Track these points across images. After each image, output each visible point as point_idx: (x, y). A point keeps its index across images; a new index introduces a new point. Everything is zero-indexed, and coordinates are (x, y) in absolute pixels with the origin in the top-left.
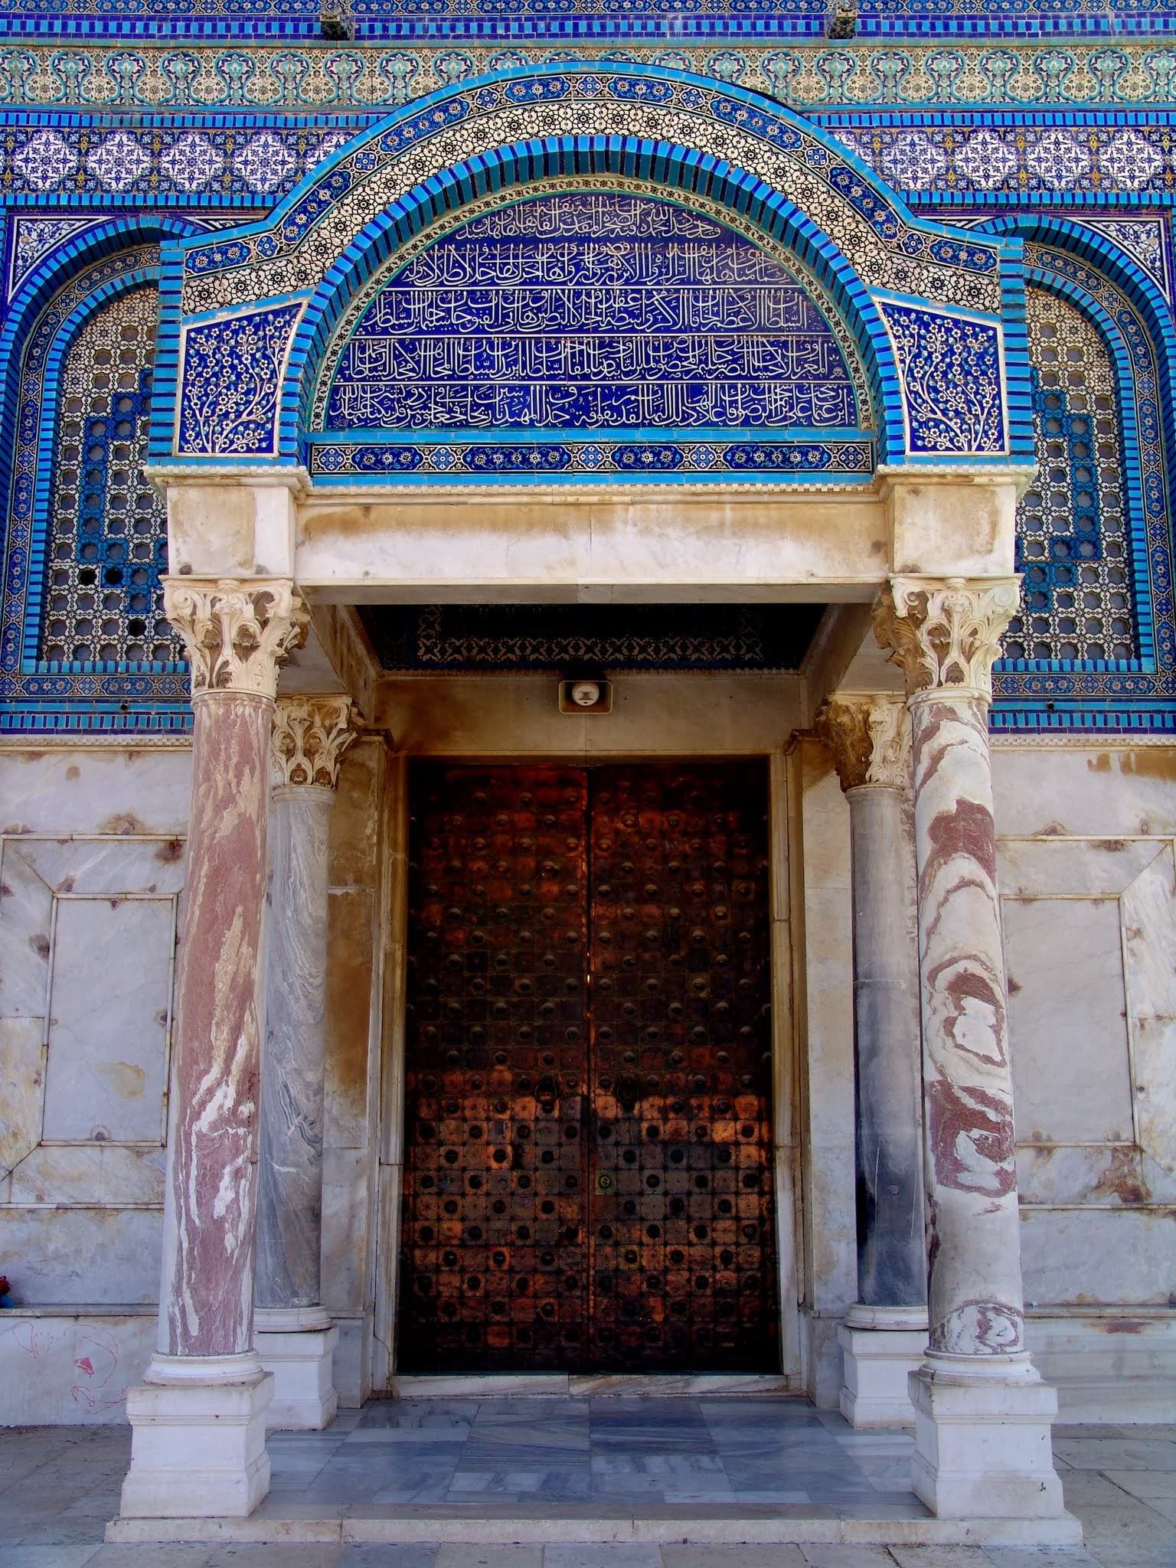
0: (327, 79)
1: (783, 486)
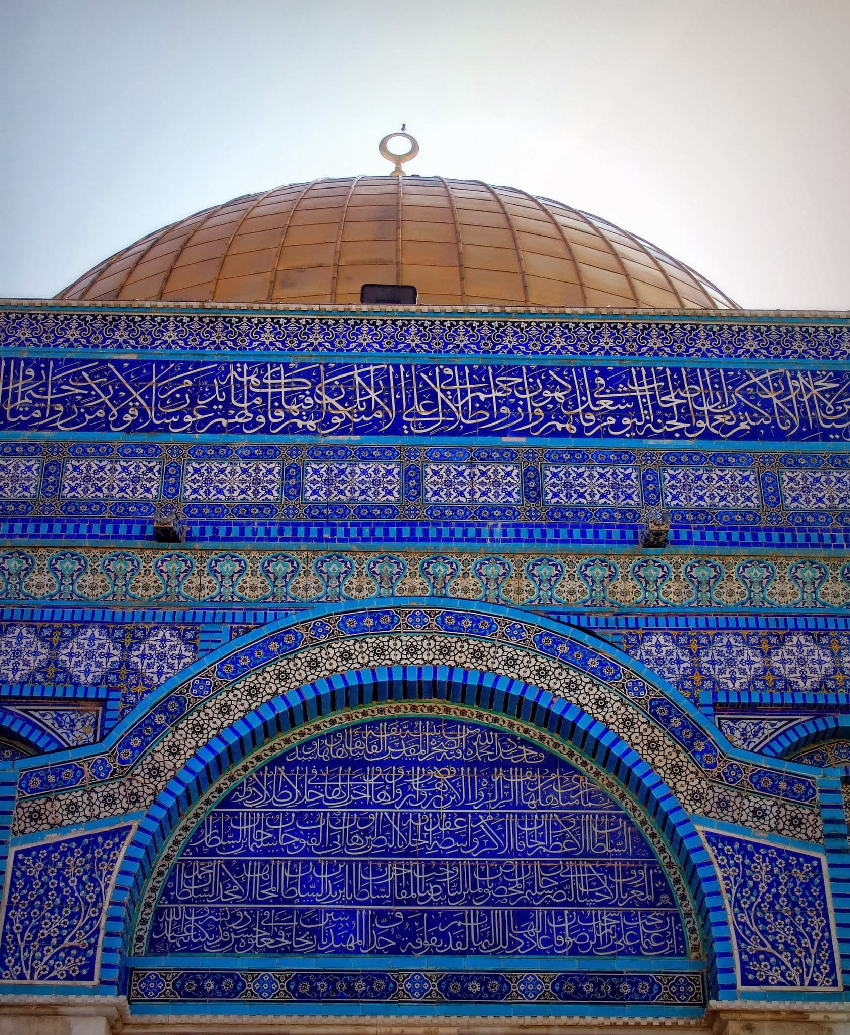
1: (613, 1019)
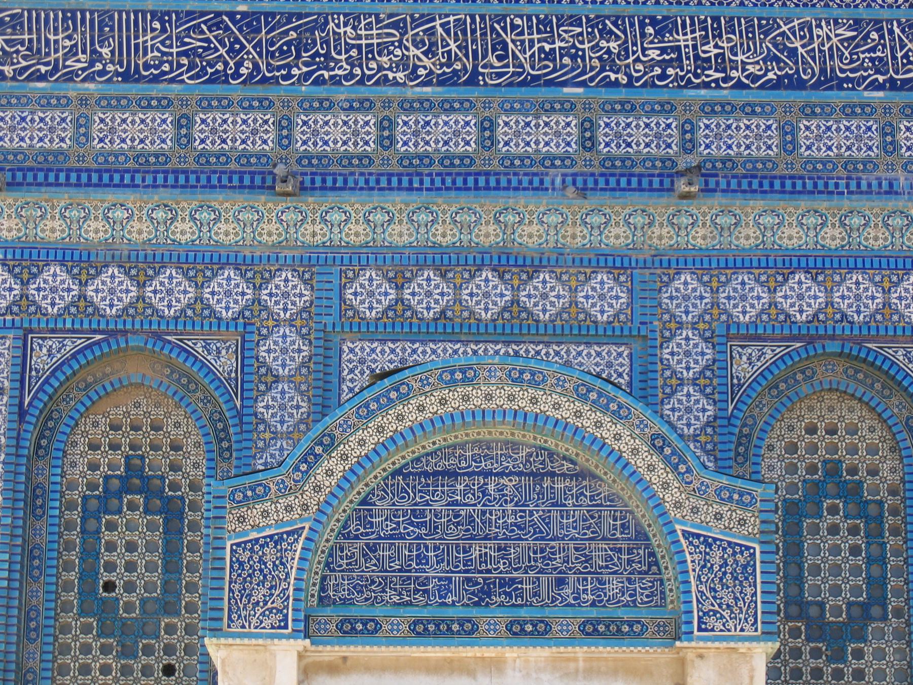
0: (278, 225)
1: (616, 648)
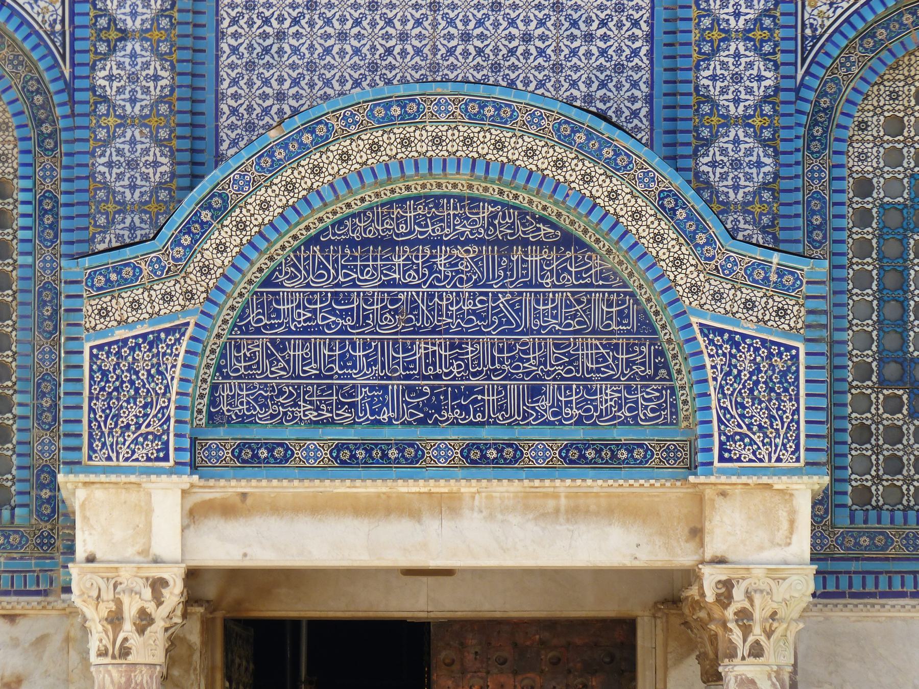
1: (611, 482)
